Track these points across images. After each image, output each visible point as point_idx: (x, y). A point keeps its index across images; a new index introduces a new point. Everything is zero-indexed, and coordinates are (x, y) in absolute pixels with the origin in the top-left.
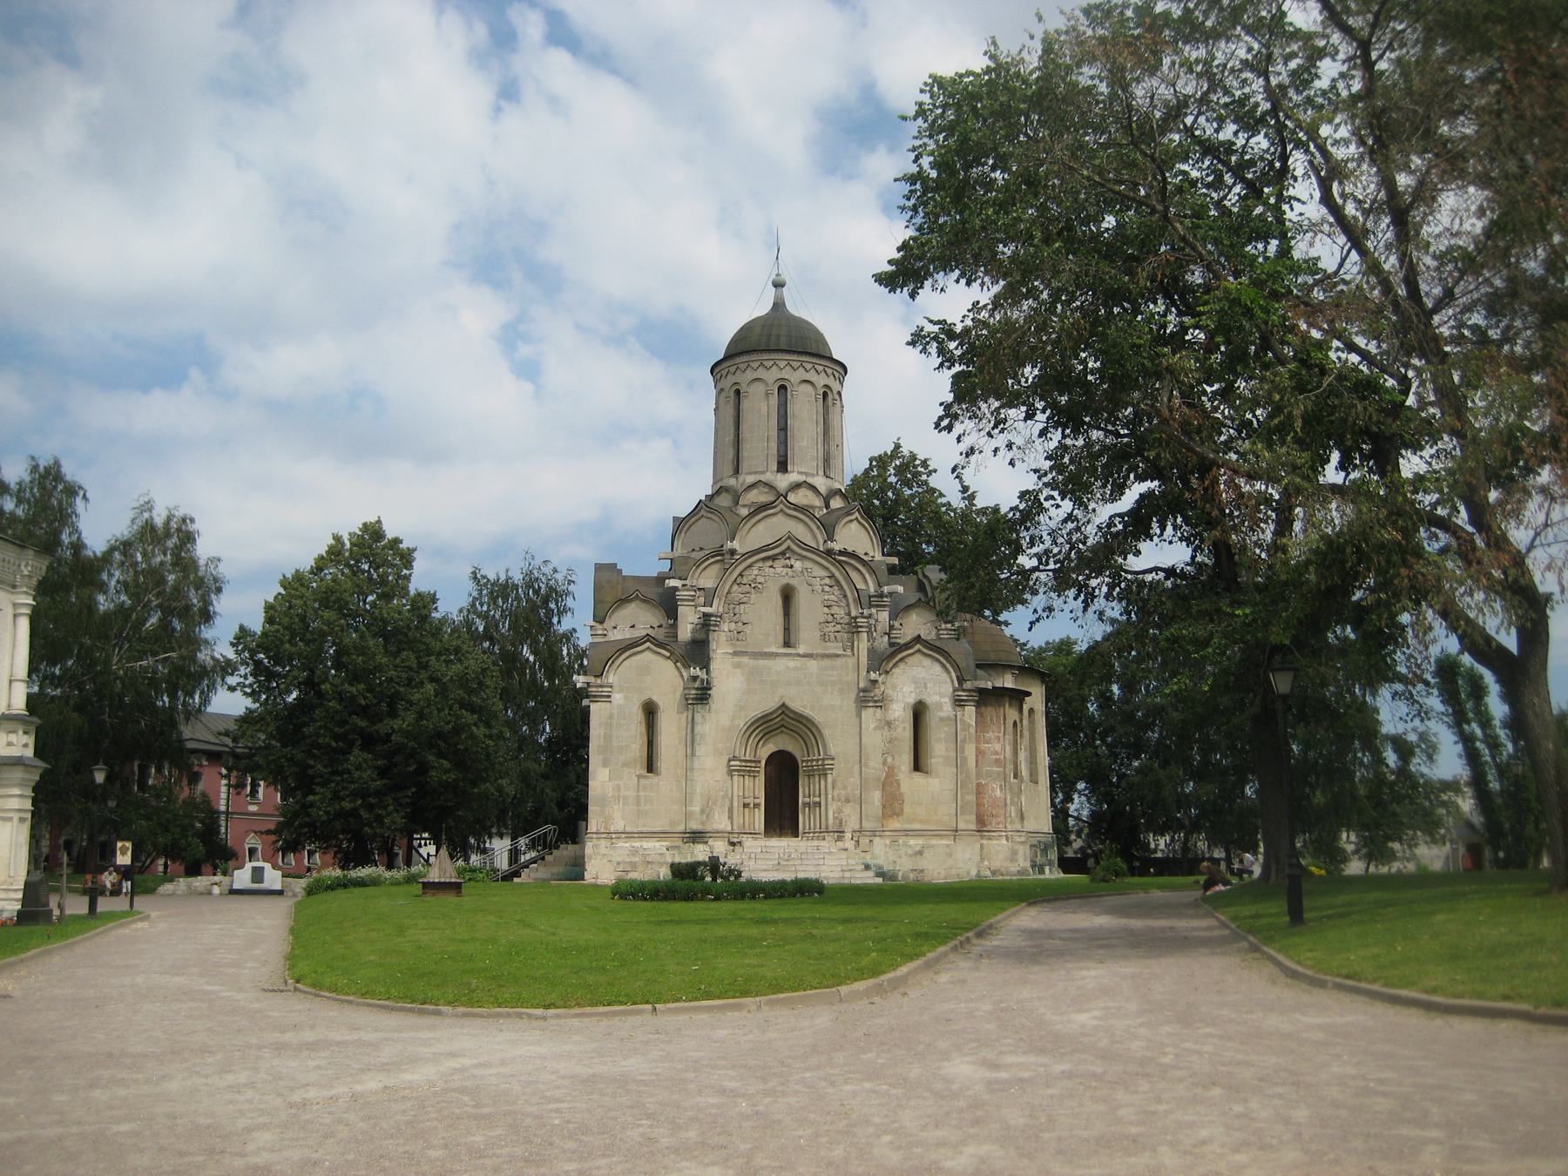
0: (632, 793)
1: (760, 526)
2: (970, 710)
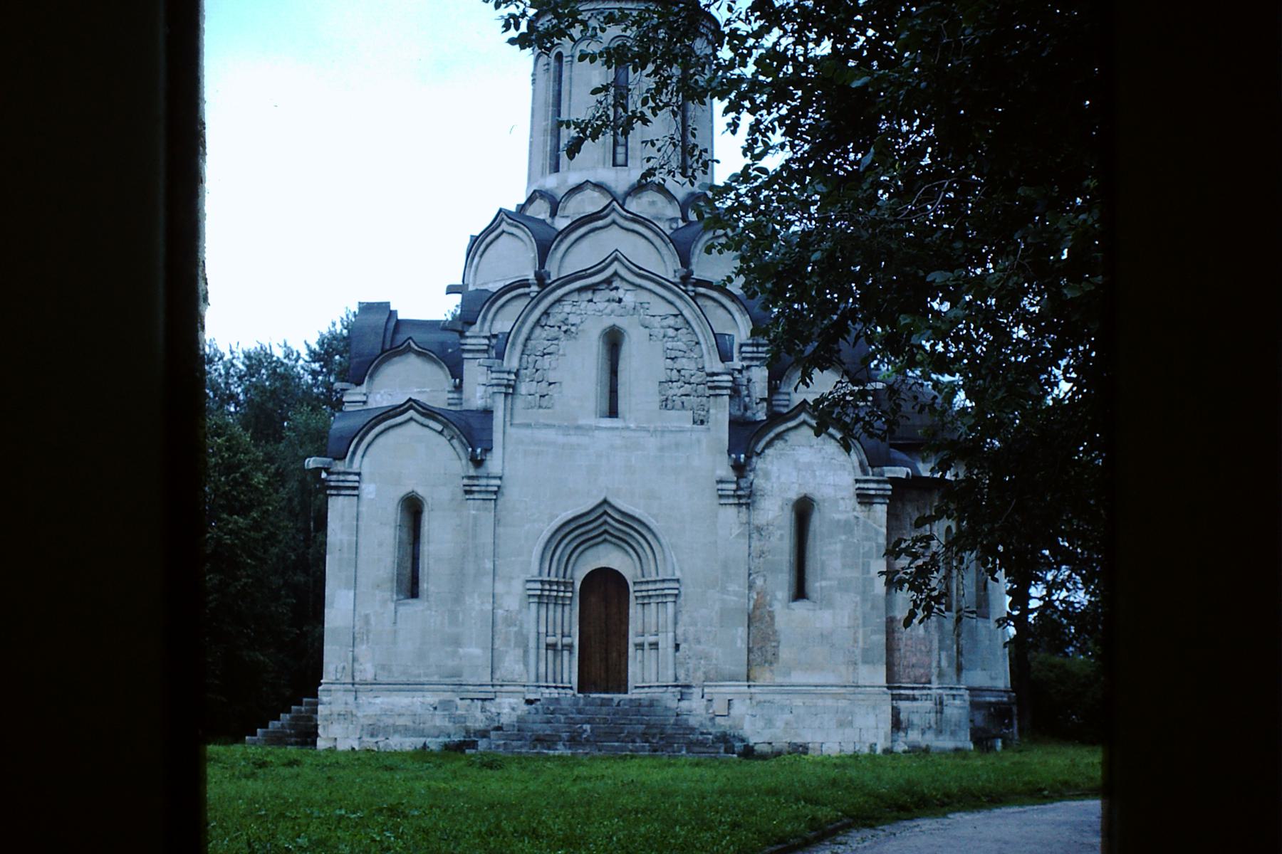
2: (881, 510)
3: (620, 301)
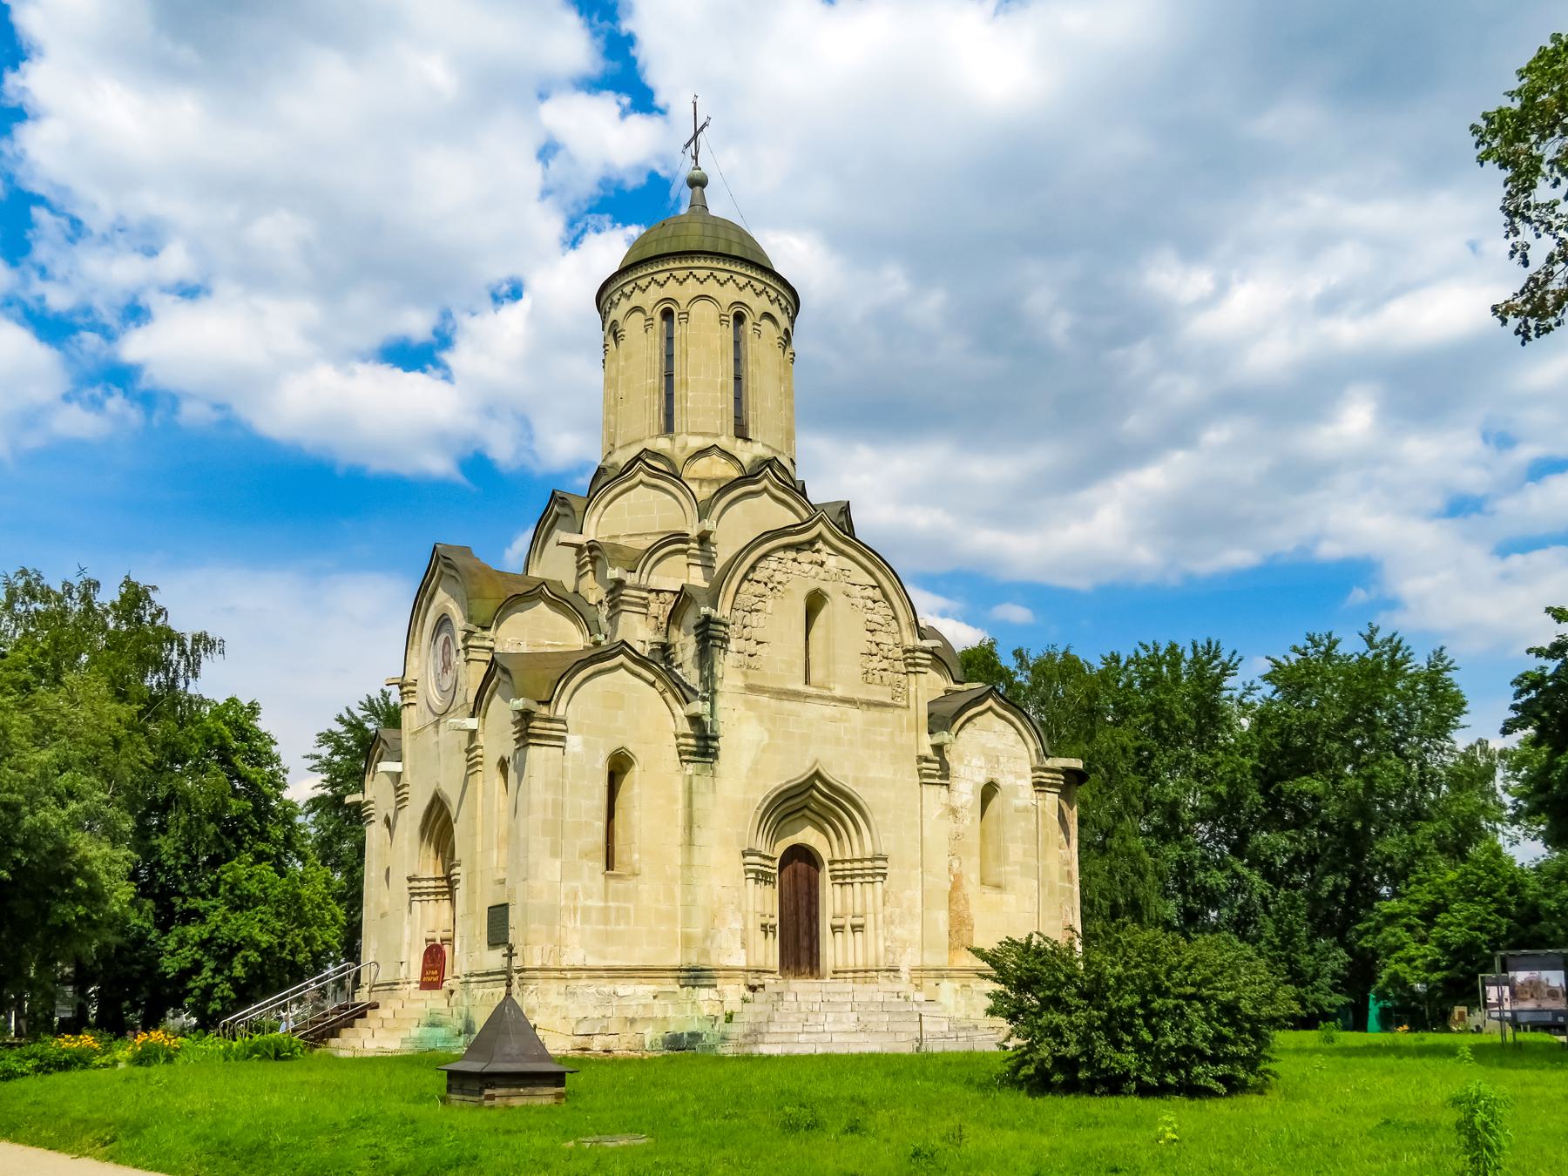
0: (597, 903)
1: (737, 507)
2: (1052, 799)
3: (822, 564)
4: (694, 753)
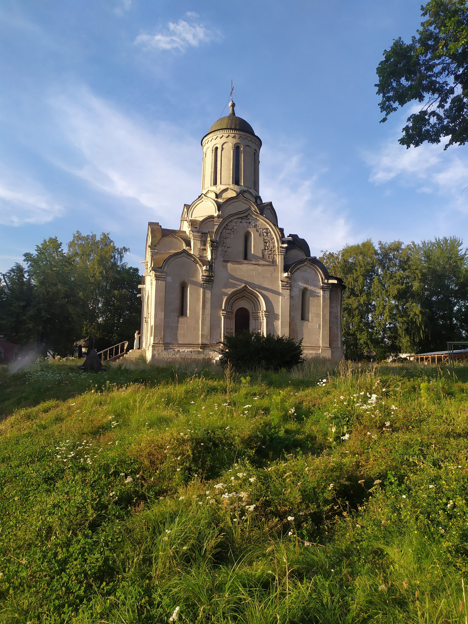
4: (206, 281)
